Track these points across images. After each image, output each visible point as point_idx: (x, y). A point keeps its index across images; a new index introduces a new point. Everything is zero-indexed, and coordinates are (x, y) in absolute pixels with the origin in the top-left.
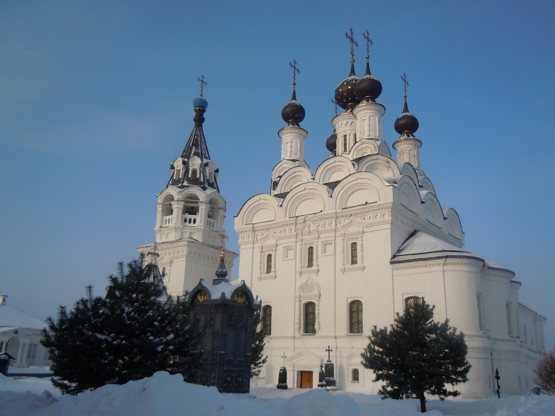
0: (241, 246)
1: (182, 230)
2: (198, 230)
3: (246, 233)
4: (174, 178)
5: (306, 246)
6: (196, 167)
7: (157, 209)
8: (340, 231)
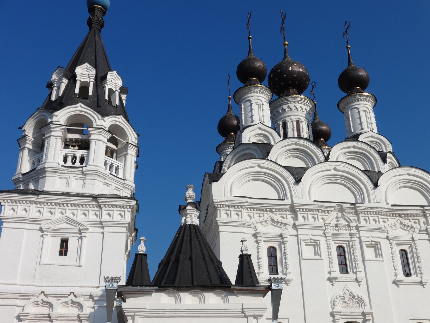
0: (220, 226)
1: (105, 179)
3: (232, 209)
4: (75, 92)
5: (346, 243)
6: (114, 89)
8: (384, 232)
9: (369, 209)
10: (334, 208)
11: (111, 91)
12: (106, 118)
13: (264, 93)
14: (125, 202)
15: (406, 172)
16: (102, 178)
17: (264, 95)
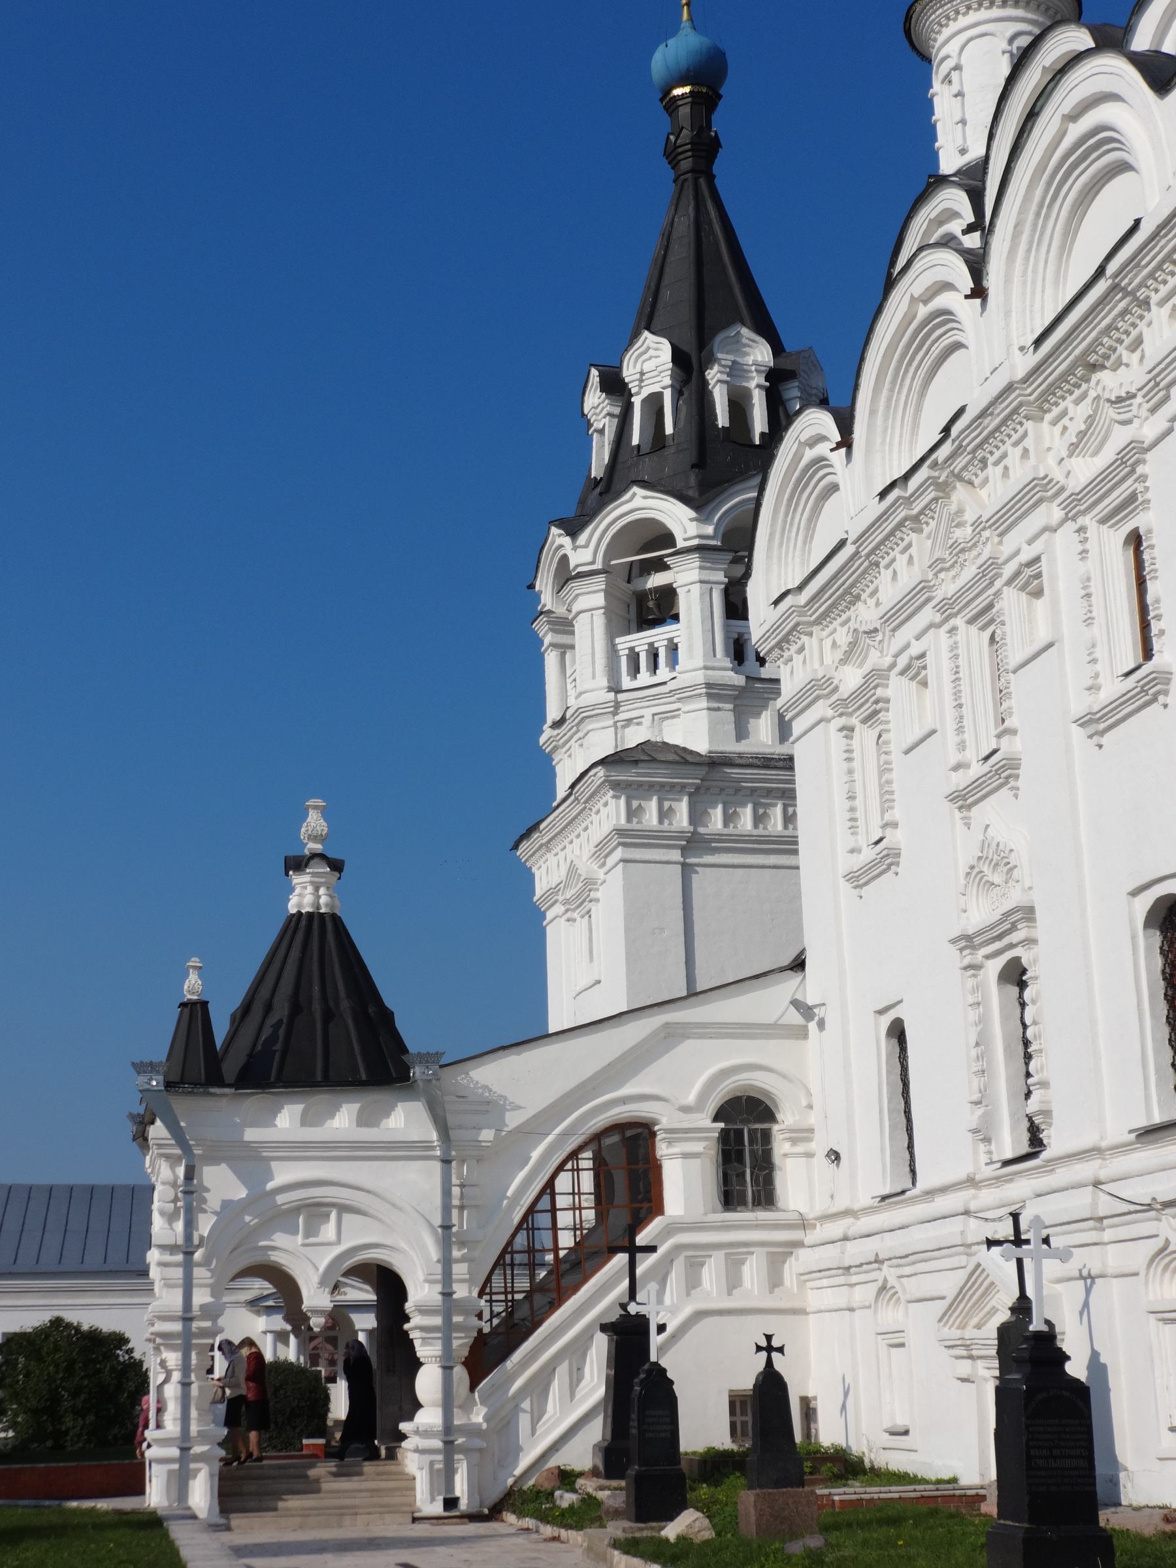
1: (615, 713)
2: (684, 694)
6: (656, 388)
7: (541, 642)
9: (986, 421)
10: (932, 488)
11: (654, 402)
12: (582, 538)
13: (948, 18)
14: (596, 779)
15: (1057, 120)
16: (605, 716)
17: (964, 14)
